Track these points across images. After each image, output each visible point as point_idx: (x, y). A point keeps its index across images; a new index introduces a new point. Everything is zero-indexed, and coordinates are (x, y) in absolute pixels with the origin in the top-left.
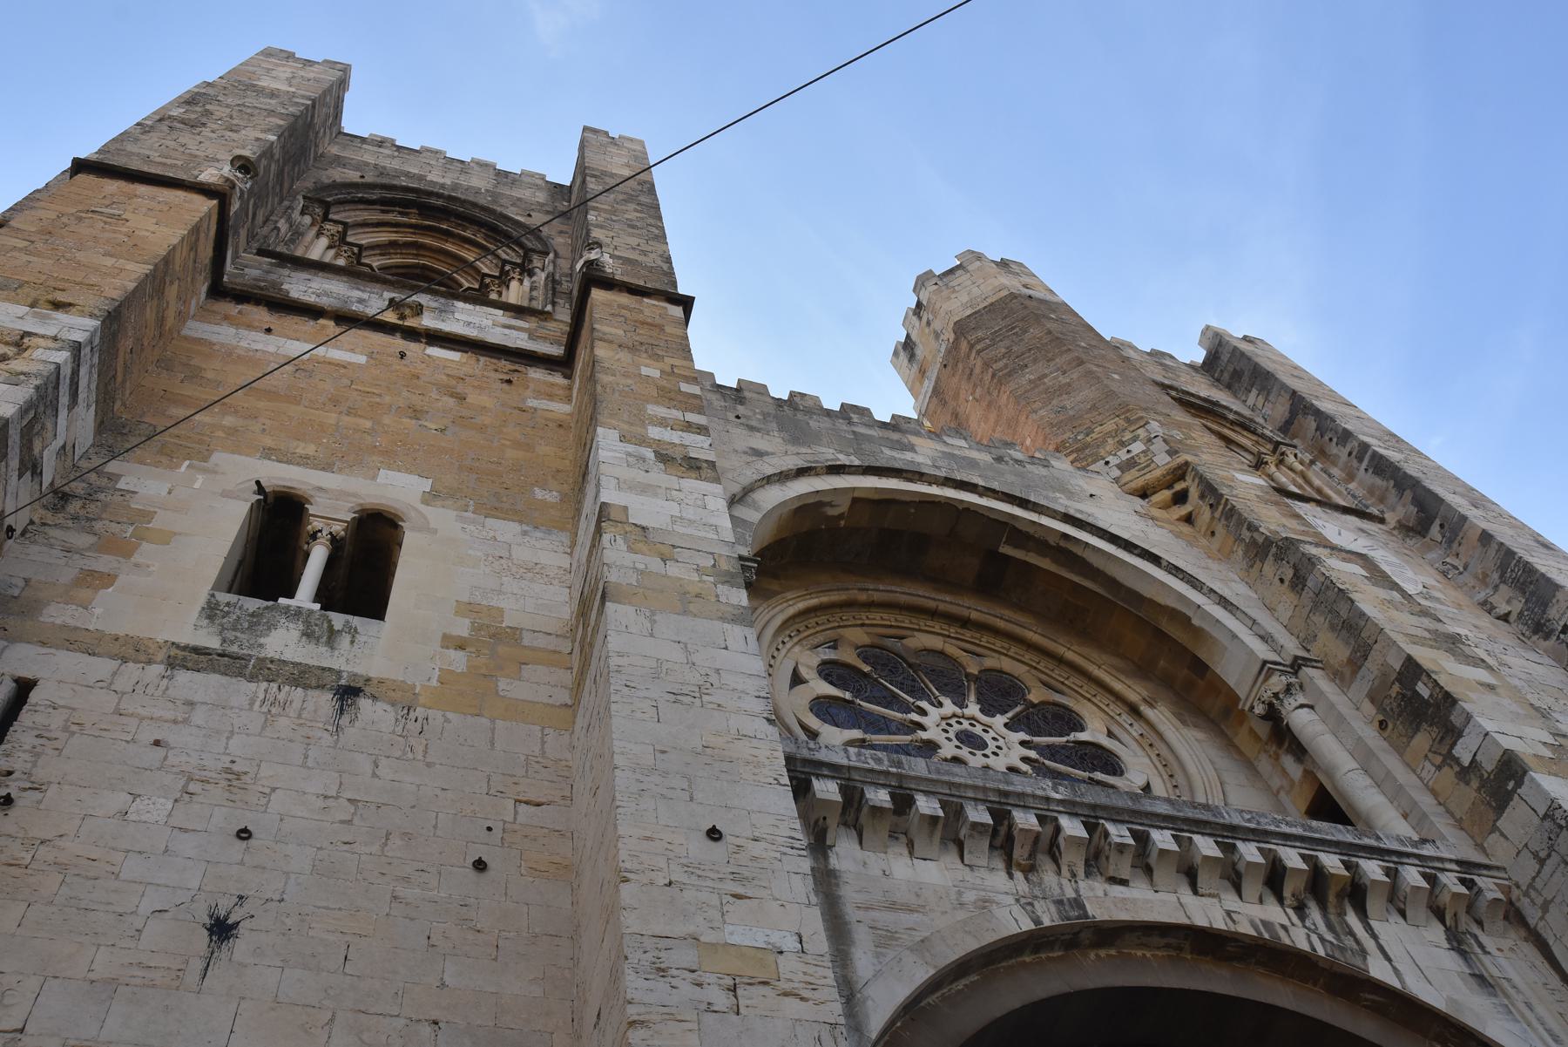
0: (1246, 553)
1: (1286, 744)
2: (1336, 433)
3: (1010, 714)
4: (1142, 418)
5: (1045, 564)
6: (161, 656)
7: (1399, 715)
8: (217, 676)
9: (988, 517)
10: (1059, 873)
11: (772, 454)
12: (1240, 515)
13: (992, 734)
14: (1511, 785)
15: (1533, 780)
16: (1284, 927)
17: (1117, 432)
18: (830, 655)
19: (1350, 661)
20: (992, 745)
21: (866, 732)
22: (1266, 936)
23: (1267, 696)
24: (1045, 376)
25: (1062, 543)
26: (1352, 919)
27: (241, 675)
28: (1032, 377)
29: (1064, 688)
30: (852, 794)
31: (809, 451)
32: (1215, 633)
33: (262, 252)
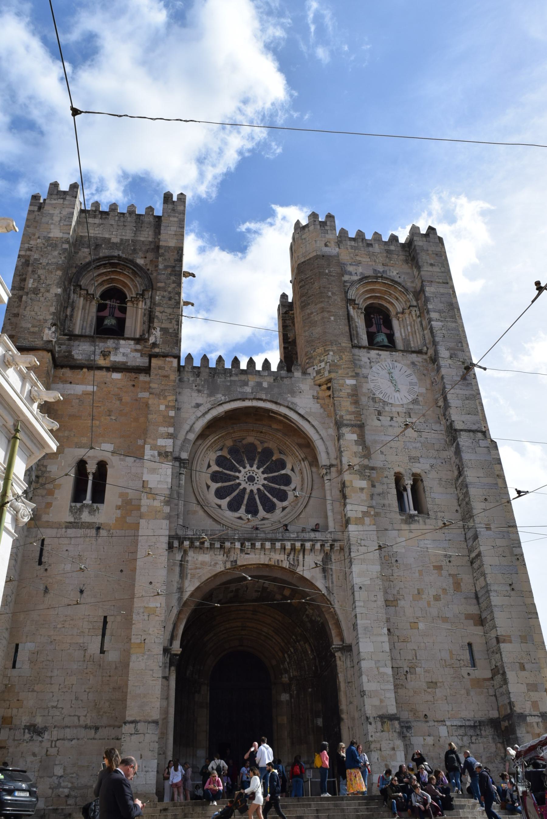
3: (265, 467)
4: (328, 350)
5: (282, 418)
6: (64, 526)
8: (74, 530)
11: (203, 404)
13: (258, 476)
16: (282, 561)
17: (320, 355)
18: (219, 453)
20: (256, 479)
21: (222, 482)
22: (276, 564)
24: (312, 313)
27: (78, 528)
30: (192, 543)
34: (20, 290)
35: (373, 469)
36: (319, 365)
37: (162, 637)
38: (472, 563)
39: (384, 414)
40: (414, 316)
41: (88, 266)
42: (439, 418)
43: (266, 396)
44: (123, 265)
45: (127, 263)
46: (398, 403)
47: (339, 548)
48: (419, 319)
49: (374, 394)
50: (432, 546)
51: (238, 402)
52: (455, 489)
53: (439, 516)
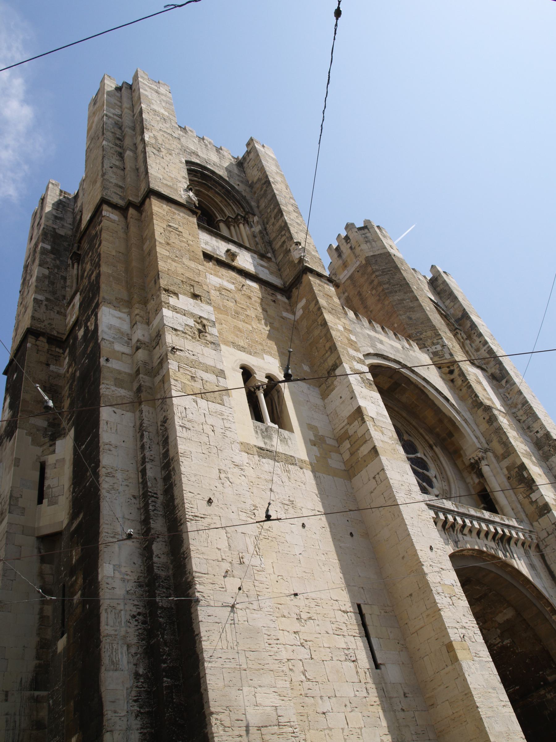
0: (472, 403)
1: (475, 470)
2: (477, 332)
7: (515, 478)
9: (403, 375)
10: (454, 532)
12: (473, 389)
14: (546, 512)
15: (553, 513)
19: (502, 454)
23: (477, 458)
24: (404, 300)
25: (422, 388)
26: (507, 546)
28: (399, 298)
29: (411, 435)
32: (466, 435)
36: (434, 347)
40: (460, 338)
48: (468, 342)
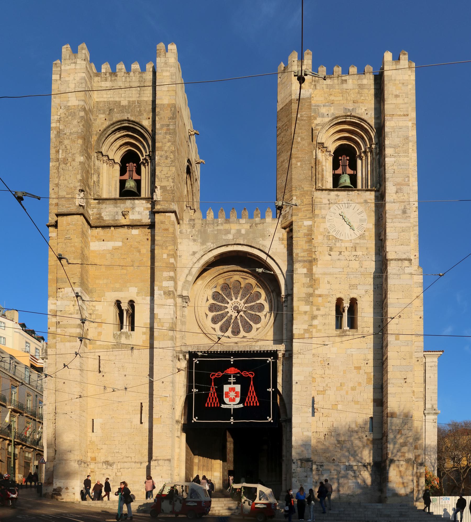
31: (206, 246)
33: (95, 199)
34: (57, 161)
35: (320, 296)
37: (171, 414)
38: (383, 364)
39: (334, 249)
41: (105, 132)
42: (379, 251)
43: (243, 241)
44: (133, 128)
45: (135, 125)
46: (347, 239)
47: (288, 356)
49: (329, 233)
50: (356, 353)
51: (223, 247)
52: (381, 309)
53: (365, 331)
